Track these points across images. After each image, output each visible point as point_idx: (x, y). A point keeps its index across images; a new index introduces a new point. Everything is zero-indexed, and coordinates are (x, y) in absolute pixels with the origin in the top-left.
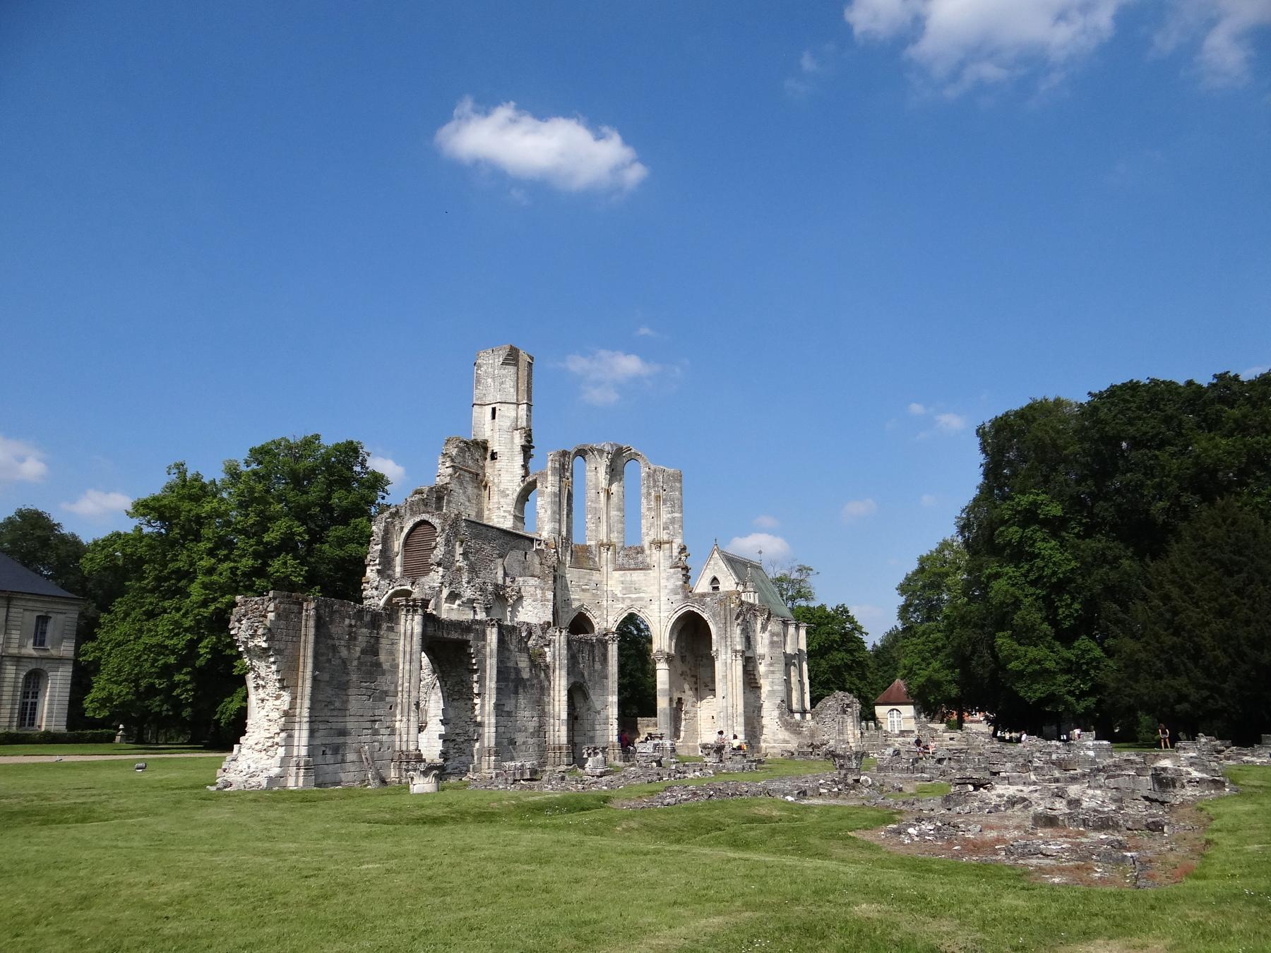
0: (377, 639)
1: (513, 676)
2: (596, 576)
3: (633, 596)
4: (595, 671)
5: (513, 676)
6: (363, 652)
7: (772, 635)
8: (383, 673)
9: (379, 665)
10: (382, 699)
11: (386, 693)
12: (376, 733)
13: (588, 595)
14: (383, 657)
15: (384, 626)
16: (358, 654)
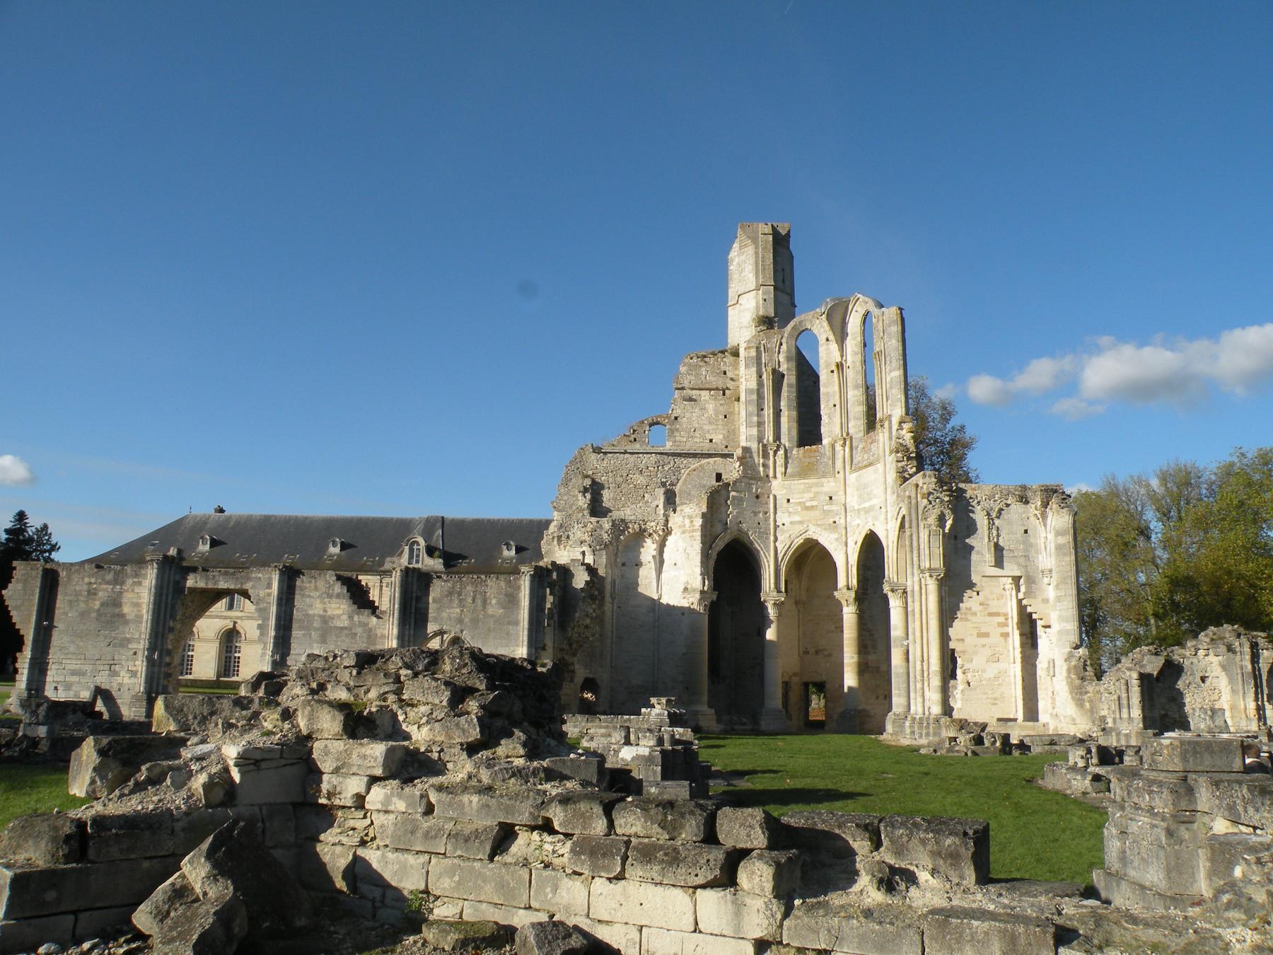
0: (121, 593)
1: (316, 624)
2: (829, 485)
3: (867, 505)
4: (486, 616)
5: (316, 624)
6: (102, 604)
7: (1058, 533)
8: (126, 622)
9: (122, 616)
10: (122, 646)
11: (129, 641)
12: (116, 674)
13: (816, 513)
14: (126, 609)
15: (129, 581)
16: (96, 607)
